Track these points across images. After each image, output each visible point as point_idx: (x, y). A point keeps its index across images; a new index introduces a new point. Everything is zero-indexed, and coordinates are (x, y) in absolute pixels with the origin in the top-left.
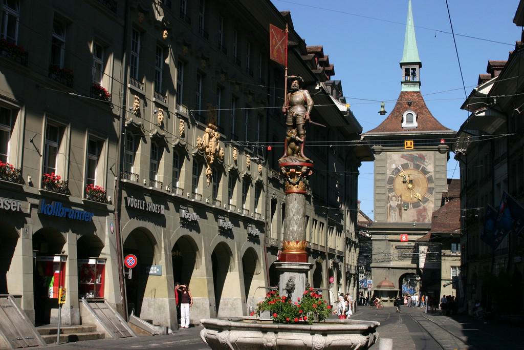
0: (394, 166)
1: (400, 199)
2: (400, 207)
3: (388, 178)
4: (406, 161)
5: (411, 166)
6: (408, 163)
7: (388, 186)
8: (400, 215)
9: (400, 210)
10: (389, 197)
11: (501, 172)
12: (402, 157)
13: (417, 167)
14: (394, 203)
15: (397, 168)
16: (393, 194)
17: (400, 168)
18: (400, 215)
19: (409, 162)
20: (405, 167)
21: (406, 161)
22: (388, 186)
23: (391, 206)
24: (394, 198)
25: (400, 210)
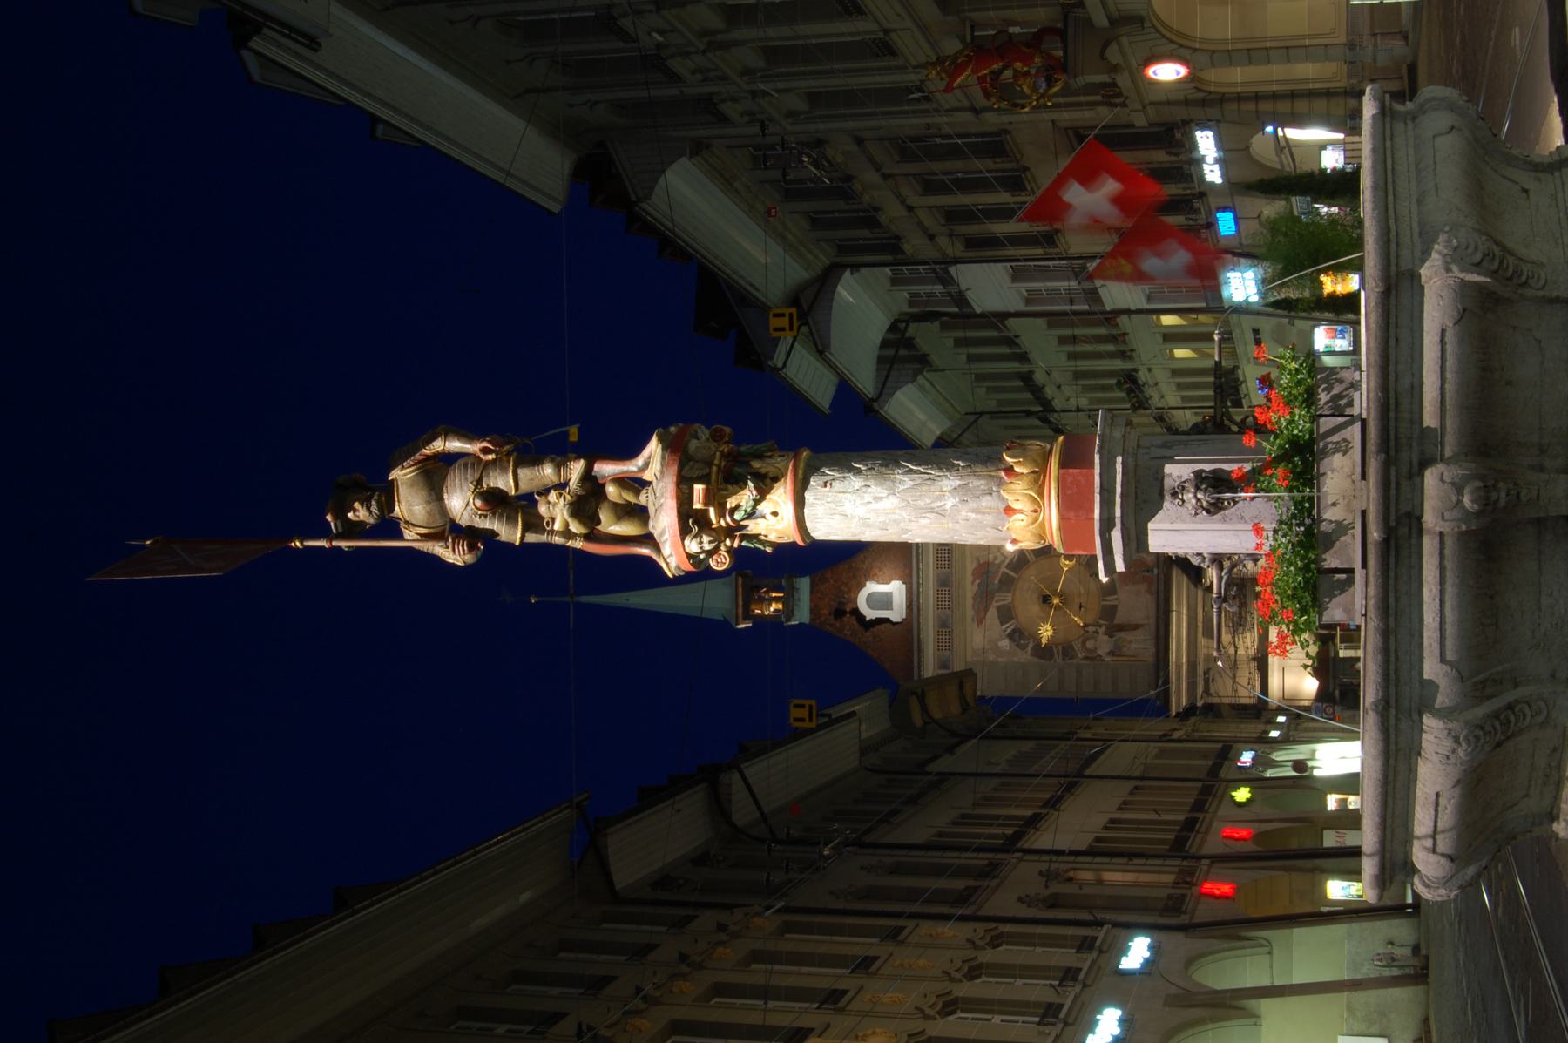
0: (1005, 643)
1: (1091, 629)
2: (1114, 629)
3: (1036, 660)
4: (992, 613)
5: (1004, 598)
6: (999, 609)
7: (1058, 659)
8: (1136, 627)
9: (1121, 628)
10: (1086, 658)
11: (989, 286)
12: (980, 621)
13: (1007, 583)
14: (1103, 644)
15: (1011, 636)
16: (1077, 645)
17: (1009, 627)
18: (1136, 627)
19: (995, 604)
20: (1006, 614)
21: (992, 613)
22: (1058, 659)
23: (1111, 653)
24: (1090, 644)
25: (1121, 628)
